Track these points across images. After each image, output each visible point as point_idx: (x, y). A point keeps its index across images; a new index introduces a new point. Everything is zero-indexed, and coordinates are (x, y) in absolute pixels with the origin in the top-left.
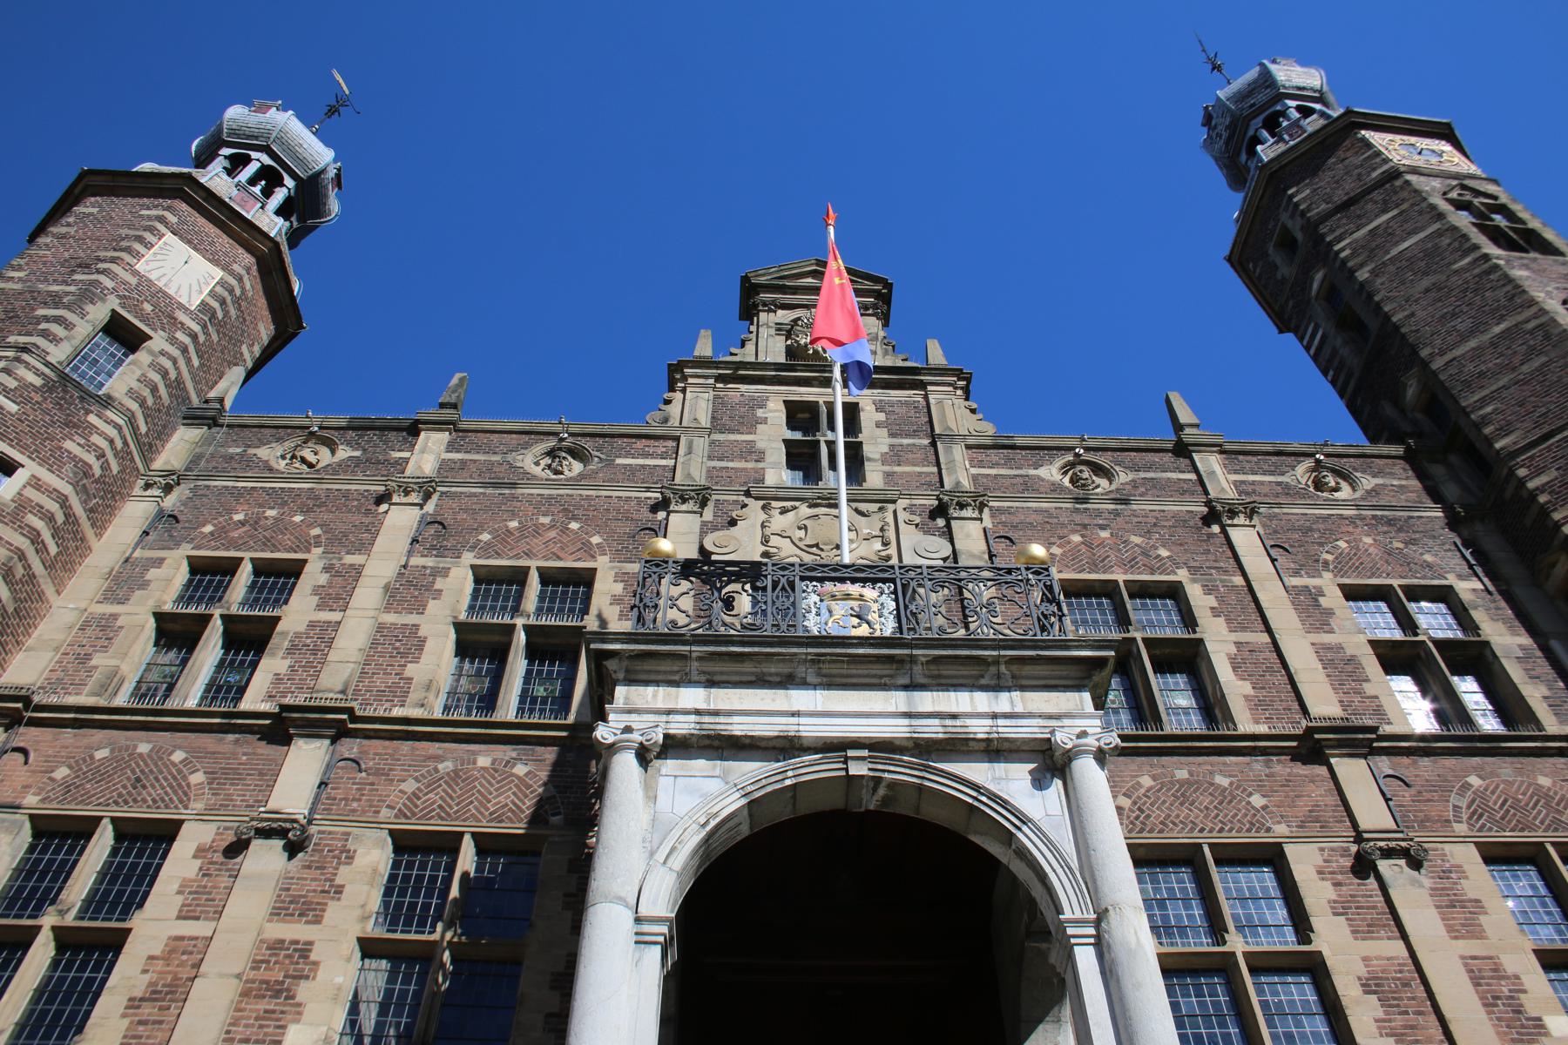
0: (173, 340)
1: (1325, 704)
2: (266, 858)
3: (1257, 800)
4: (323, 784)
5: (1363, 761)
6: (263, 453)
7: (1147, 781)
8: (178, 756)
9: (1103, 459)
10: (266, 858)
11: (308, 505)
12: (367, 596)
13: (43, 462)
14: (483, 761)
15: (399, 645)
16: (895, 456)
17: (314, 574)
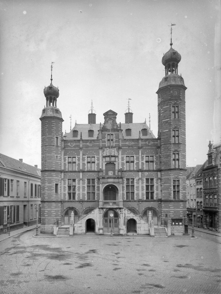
0: (60, 136)
1: (140, 168)
2: (81, 181)
3: (134, 175)
4: (82, 176)
5: (141, 173)
6: (69, 144)
7: (128, 174)
8: (74, 174)
9: (131, 141)
10: (81, 181)
11: (74, 150)
12: (81, 160)
13: (58, 155)
14: (91, 174)
15: (84, 164)
16: (116, 141)
17: (77, 158)
